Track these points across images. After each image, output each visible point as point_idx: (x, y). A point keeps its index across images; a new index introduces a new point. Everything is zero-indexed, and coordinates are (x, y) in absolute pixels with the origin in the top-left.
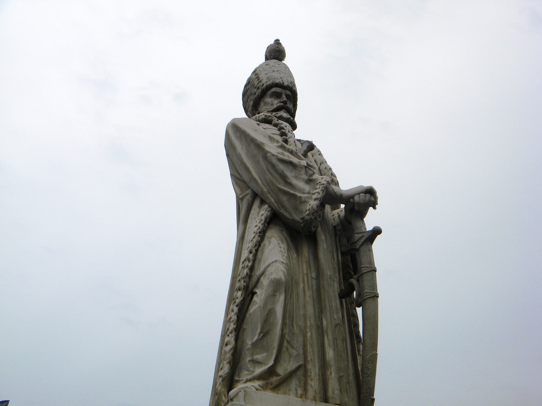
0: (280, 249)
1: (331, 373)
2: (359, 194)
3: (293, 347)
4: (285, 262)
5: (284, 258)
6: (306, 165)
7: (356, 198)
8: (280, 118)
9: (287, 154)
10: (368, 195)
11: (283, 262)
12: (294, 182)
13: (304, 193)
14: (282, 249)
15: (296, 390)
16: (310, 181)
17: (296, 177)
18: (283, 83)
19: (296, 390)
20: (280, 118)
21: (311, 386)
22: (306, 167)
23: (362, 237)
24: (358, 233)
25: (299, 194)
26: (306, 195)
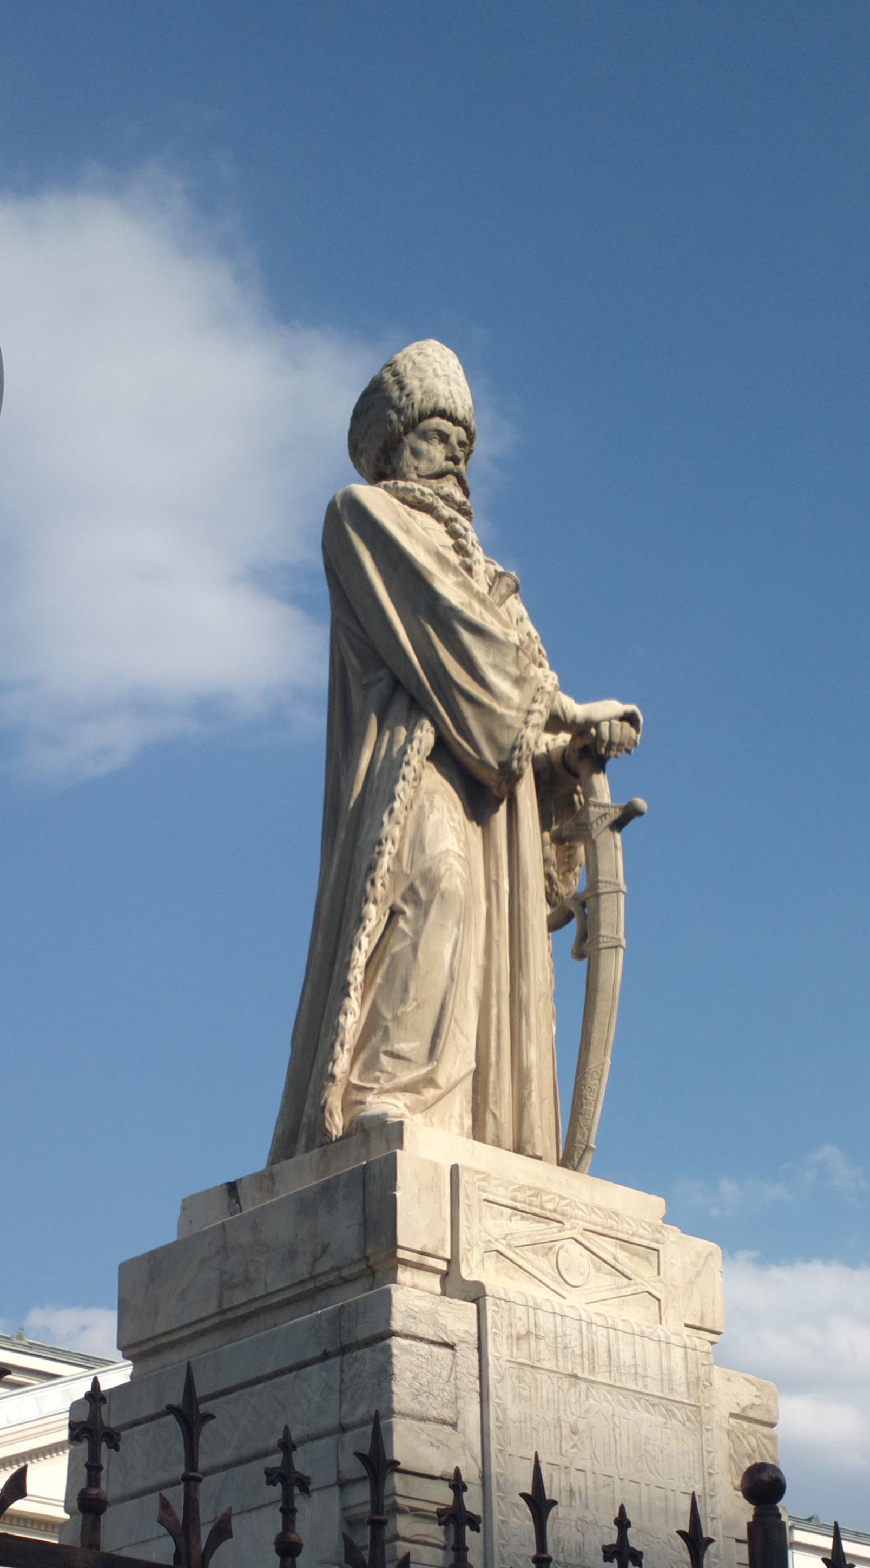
0: (452, 824)
1: (530, 1094)
2: (609, 720)
3: (462, 1033)
4: (463, 855)
5: (461, 845)
6: (518, 643)
7: (605, 728)
8: (448, 499)
9: (477, 606)
10: (626, 725)
11: (459, 855)
12: (492, 677)
13: (509, 707)
14: (456, 825)
15: (462, 1118)
16: (519, 681)
17: (495, 667)
18: (456, 410)
19: (462, 1118)
20: (448, 499)
21: (494, 1115)
22: (518, 648)
23: (605, 815)
24: (595, 805)
25: (500, 709)
26: (513, 713)
